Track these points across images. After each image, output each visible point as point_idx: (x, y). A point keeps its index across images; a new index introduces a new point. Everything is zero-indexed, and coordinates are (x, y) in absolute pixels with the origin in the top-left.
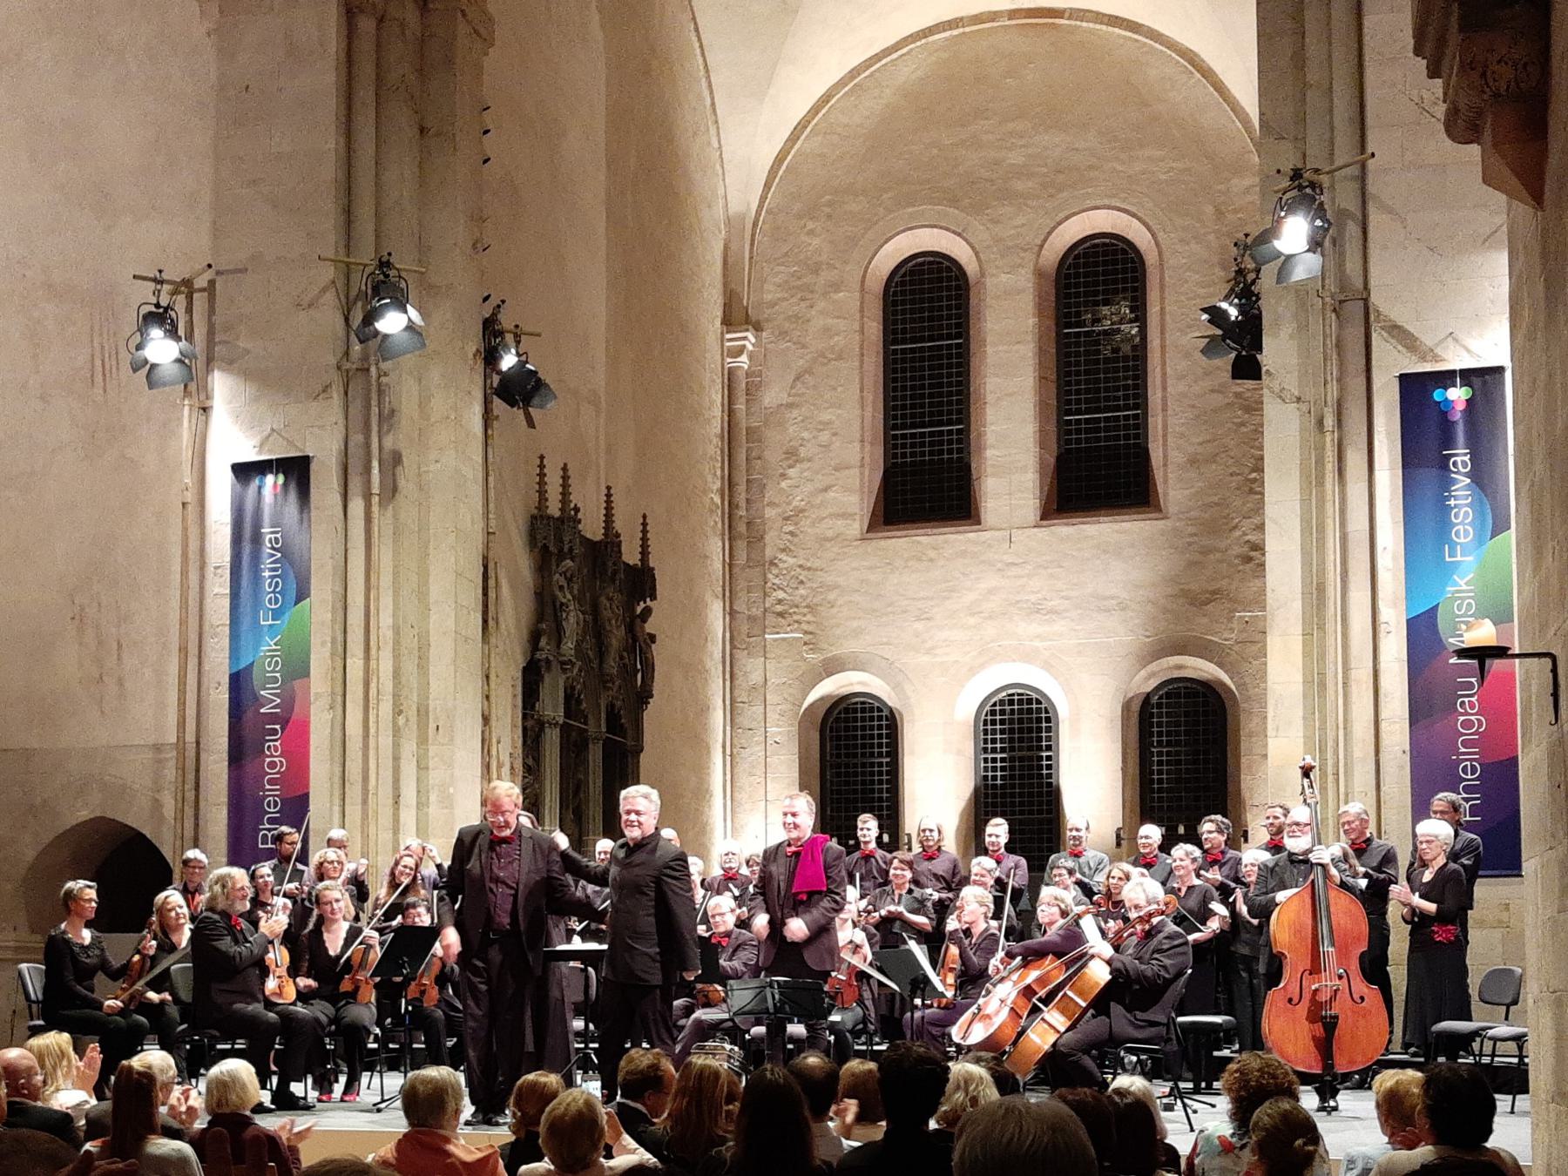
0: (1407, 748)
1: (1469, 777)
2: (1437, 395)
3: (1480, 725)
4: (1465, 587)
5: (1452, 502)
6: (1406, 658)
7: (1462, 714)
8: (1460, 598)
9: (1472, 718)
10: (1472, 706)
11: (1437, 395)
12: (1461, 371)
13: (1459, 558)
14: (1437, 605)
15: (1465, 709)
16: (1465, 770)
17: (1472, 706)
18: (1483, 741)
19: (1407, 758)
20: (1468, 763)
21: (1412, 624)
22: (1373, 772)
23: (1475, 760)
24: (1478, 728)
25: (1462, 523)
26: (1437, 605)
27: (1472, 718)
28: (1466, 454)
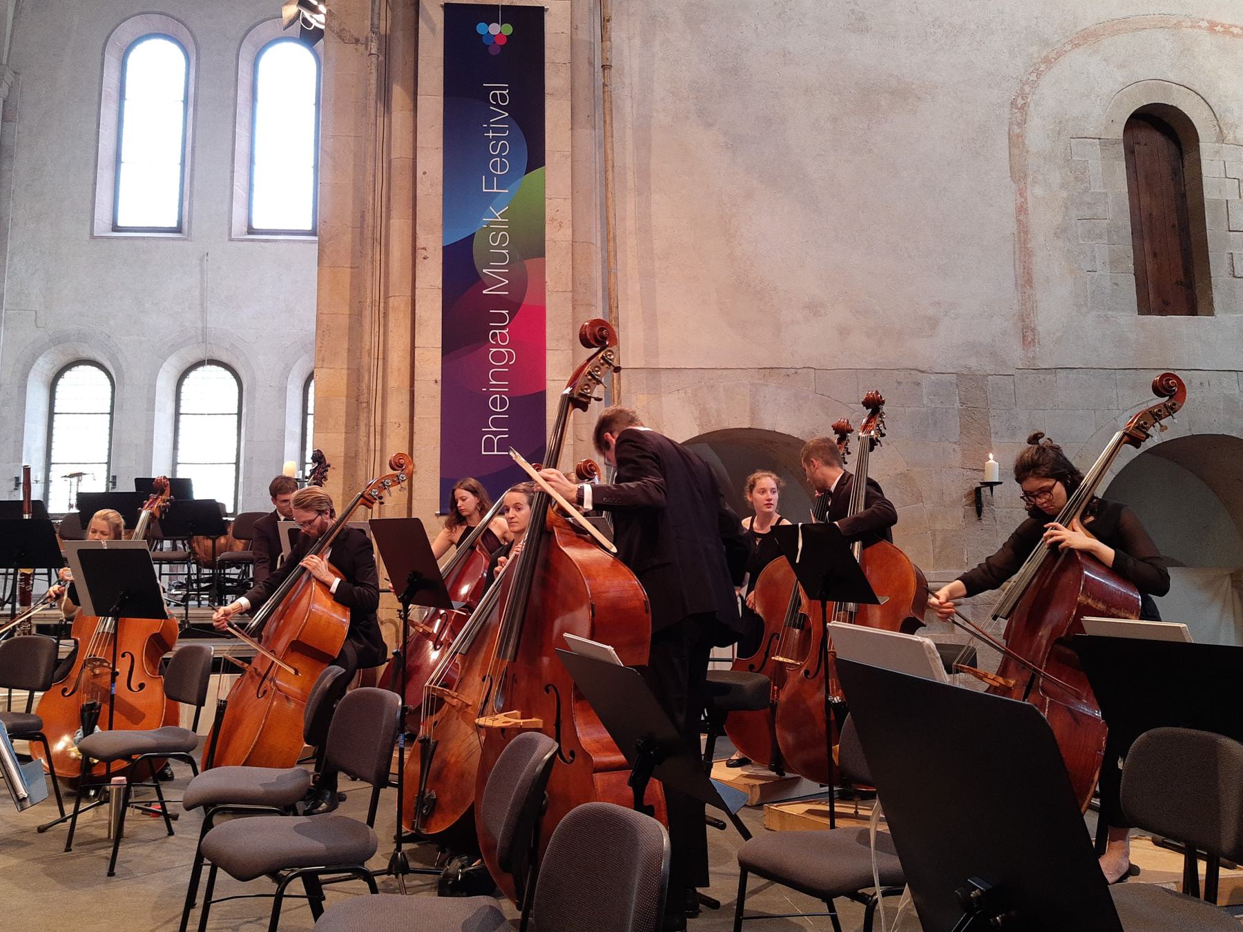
0: (439, 378)
1: (498, 410)
2: (481, 28)
3: (510, 358)
4: (500, 220)
5: (491, 135)
6: (441, 287)
7: (494, 346)
8: (493, 230)
9: (503, 350)
10: (503, 338)
11: (481, 28)
12: (502, 6)
13: (495, 190)
14: (474, 234)
15: (497, 341)
16: (494, 403)
17: (503, 338)
18: (511, 375)
19: (438, 388)
20: (498, 396)
21: (447, 251)
22: (407, 403)
23: (504, 393)
24: (509, 361)
25: (499, 155)
26: (474, 234)
27: (503, 350)
28: (504, 89)
